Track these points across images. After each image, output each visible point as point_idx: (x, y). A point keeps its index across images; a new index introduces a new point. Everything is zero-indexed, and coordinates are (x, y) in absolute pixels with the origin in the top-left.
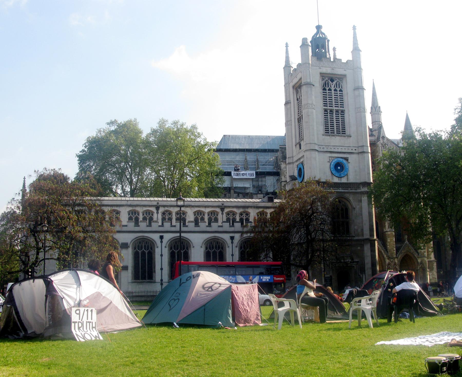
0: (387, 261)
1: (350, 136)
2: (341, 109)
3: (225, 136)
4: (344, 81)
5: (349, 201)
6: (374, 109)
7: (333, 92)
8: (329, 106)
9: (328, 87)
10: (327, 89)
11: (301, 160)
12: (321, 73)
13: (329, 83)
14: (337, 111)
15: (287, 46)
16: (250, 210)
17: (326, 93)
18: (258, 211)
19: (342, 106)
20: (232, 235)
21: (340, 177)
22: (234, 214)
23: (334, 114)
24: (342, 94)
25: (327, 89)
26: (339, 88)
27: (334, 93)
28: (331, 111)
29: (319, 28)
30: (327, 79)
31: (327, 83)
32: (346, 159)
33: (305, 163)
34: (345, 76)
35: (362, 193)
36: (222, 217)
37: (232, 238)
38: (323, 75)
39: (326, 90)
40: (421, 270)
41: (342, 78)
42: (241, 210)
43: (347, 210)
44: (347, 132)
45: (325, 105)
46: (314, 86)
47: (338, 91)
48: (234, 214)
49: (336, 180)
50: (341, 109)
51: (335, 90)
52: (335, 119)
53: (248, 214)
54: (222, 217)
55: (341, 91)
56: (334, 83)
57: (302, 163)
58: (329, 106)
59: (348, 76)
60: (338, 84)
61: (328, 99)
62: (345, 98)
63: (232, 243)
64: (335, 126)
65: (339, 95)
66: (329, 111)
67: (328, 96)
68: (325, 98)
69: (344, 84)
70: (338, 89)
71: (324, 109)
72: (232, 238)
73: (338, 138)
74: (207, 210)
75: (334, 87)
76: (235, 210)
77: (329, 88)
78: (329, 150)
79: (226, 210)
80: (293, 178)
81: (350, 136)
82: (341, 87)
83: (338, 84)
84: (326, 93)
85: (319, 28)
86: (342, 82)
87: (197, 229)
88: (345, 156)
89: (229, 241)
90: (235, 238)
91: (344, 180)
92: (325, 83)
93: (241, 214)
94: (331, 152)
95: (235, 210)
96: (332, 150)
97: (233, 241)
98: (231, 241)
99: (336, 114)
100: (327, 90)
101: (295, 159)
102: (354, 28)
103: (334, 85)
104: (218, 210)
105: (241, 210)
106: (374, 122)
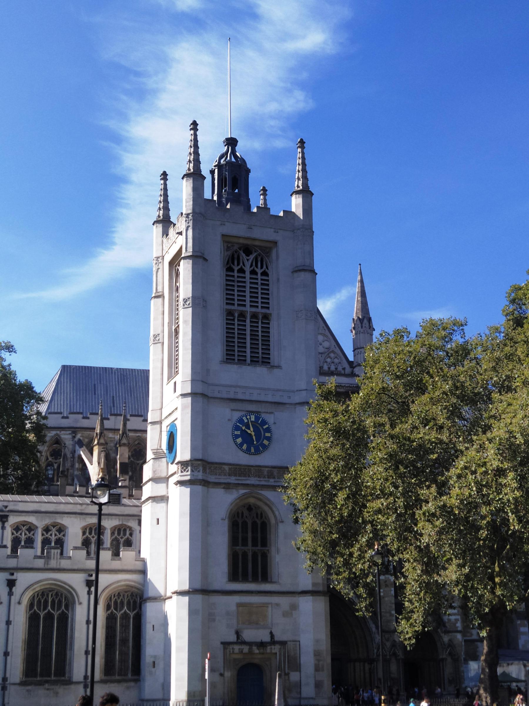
0: (378, 638)
2: (264, 311)
7: (248, 275)
8: (239, 305)
9: (238, 264)
10: (236, 268)
12: (223, 235)
13: (241, 258)
14: (254, 316)
16: (65, 521)
17: (233, 276)
18: (84, 524)
19: (266, 305)
22: (30, 530)
23: (248, 321)
24: (268, 280)
25: (236, 268)
26: (262, 267)
27: (251, 278)
30: (236, 247)
31: (236, 256)
34: (275, 243)
38: (227, 239)
39: (233, 271)
40: (449, 660)
41: (270, 249)
45: (229, 301)
46: (206, 260)
47: (259, 275)
48: (31, 528)
50: (264, 311)
51: (253, 272)
52: (248, 332)
53: (61, 529)
55: (265, 274)
56: (252, 257)
58: (239, 305)
59: (280, 244)
60: (259, 259)
61: (236, 289)
63: (10, 594)
64: (248, 345)
65: (259, 282)
66: (236, 315)
67: (236, 284)
68: (229, 288)
70: (259, 271)
71: (227, 310)
75: (251, 266)
76: (32, 519)
77: (239, 267)
82: (265, 267)
83: (259, 259)
84: (233, 276)
86: (268, 257)
90: (18, 583)
92: (233, 255)
93: (47, 530)
97: (14, 589)
98: (7, 589)
99: (251, 322)
100: (236, 271)
103: (250, 261)
105: (47, 521)
106: (358, 349)
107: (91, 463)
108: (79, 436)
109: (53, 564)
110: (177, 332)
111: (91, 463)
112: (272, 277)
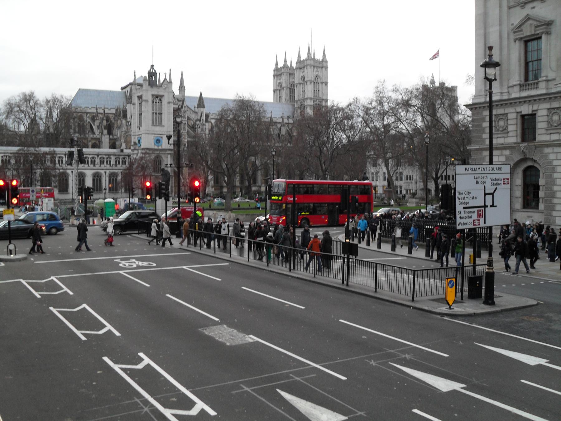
0: (182, 181)
1: (164, 126)
3: (80, 89)
4: (163, 98)
5: (162, 157)
6: (181, 88)
11: (140, 136)
14: (159, 113)
15: (135, 72)
20: (105, 171)
21: (158, 146)
28: (156, 113)
29: (152, 66)
32: (162, 137)
33: (142, 138)
35: (168, 154)
36: (97, 161)
37: (105, 172)
38: (153, 95)
42: (107, 156)
43: (161, 161)
44: (163, 124)
45: (153, 110)
48: (104, 158)
49: (156, 147)
53: (110, 158)
54: (97, 161)
55: (161, 103)
56: (158, 99)
57: (140, 137)
62: (163, 107)
68: (153, 107)
69: (163, 99)
72: (105, 172)
73: (158, 127)
74: (90, 156)
76: (104, 156)
78: (154, 133)
79: (100, 156)
80: (135, 144)
81: (164, 126)
85: (152, 66)
87: (89, 168)
88: (161, 136)
89: (104, 174)
91: (160, 148)
93: (107, 158)
94: (155, 134)
95: (104, 156)
96: (155, 133)
101: (137, 134)
102: (170, 70)
104: (96, 156)
105: (107, 156)
107: (94, 125)
108: (88, 115)
109: (114, 167)
110: (140, 114)
111: (94, 125)
112: (163, 104)
